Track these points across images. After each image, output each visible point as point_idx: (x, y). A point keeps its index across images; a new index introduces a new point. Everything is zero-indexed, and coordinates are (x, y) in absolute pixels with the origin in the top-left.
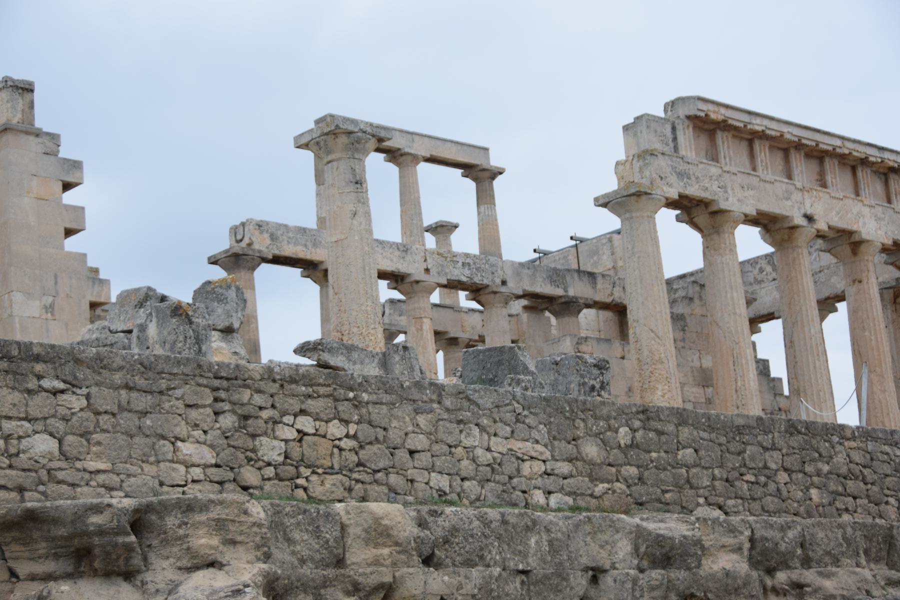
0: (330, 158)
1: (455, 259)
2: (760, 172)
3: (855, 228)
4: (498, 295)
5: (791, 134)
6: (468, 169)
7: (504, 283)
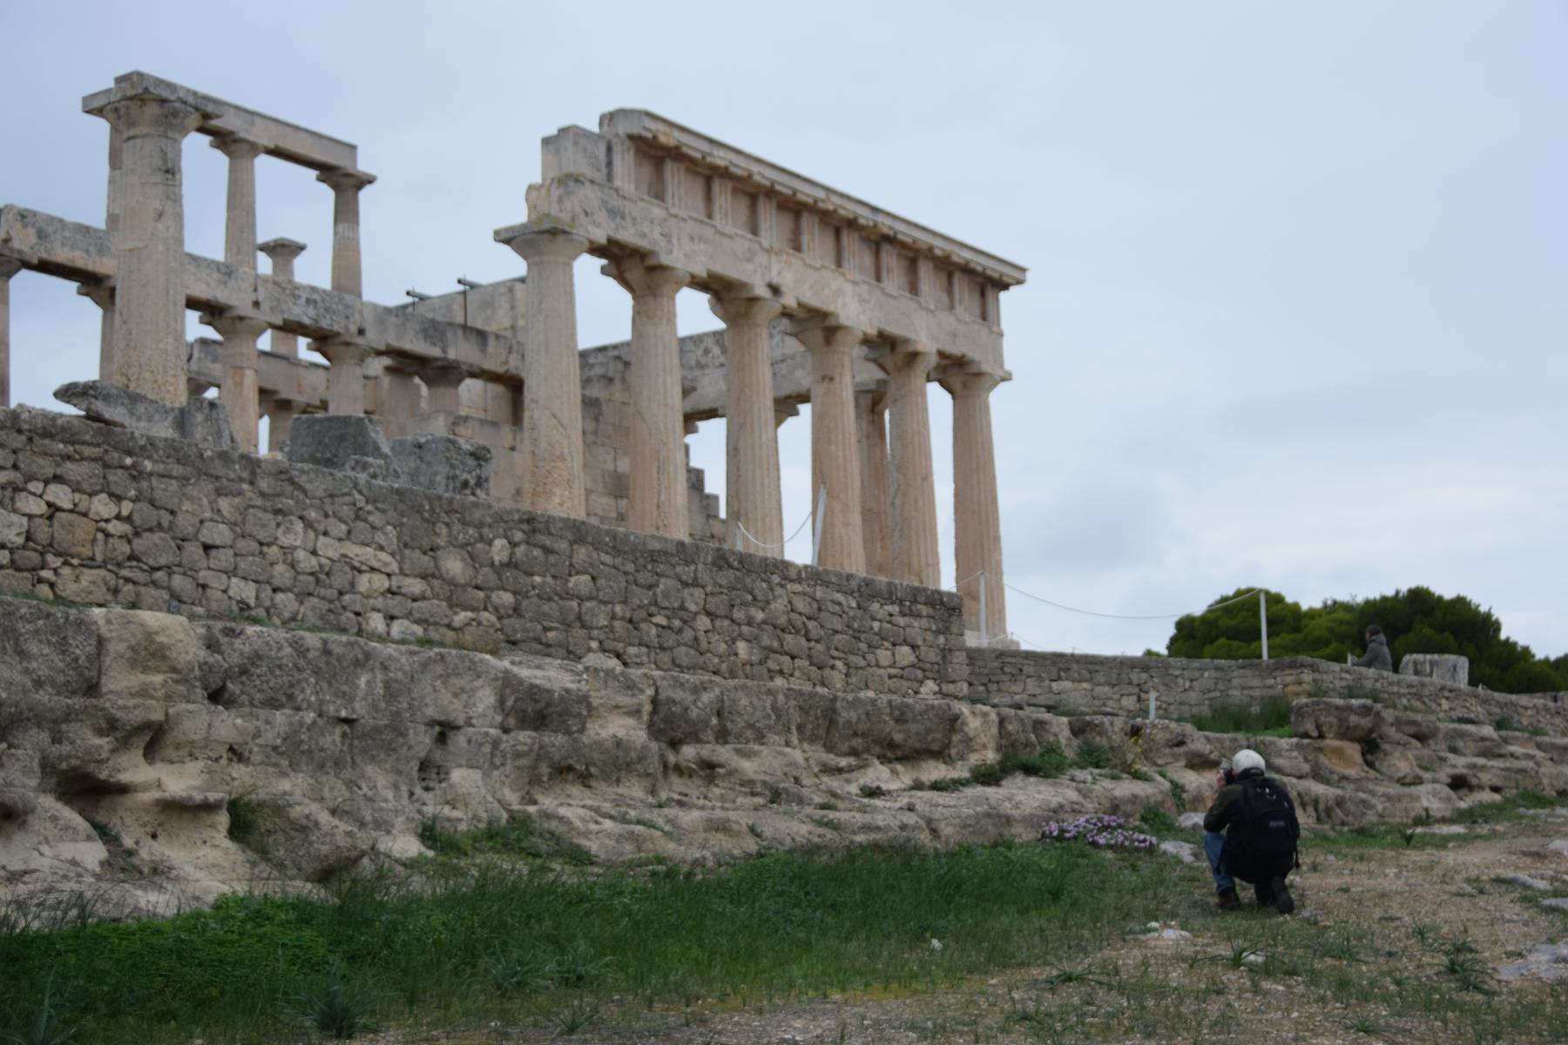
0: (132, 132)
1: (297, 292)
2: (717, 221)
3: (831, 308)
4: (351, 348)
5: (762, 176)
6: (327, 172)
7: (361, 332)
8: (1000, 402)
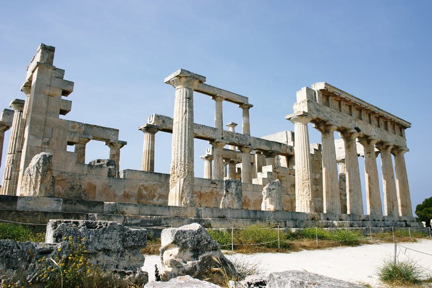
5: (353, 100)
6: (241, 104)
7: (250, 144)
8: (406, 156)
